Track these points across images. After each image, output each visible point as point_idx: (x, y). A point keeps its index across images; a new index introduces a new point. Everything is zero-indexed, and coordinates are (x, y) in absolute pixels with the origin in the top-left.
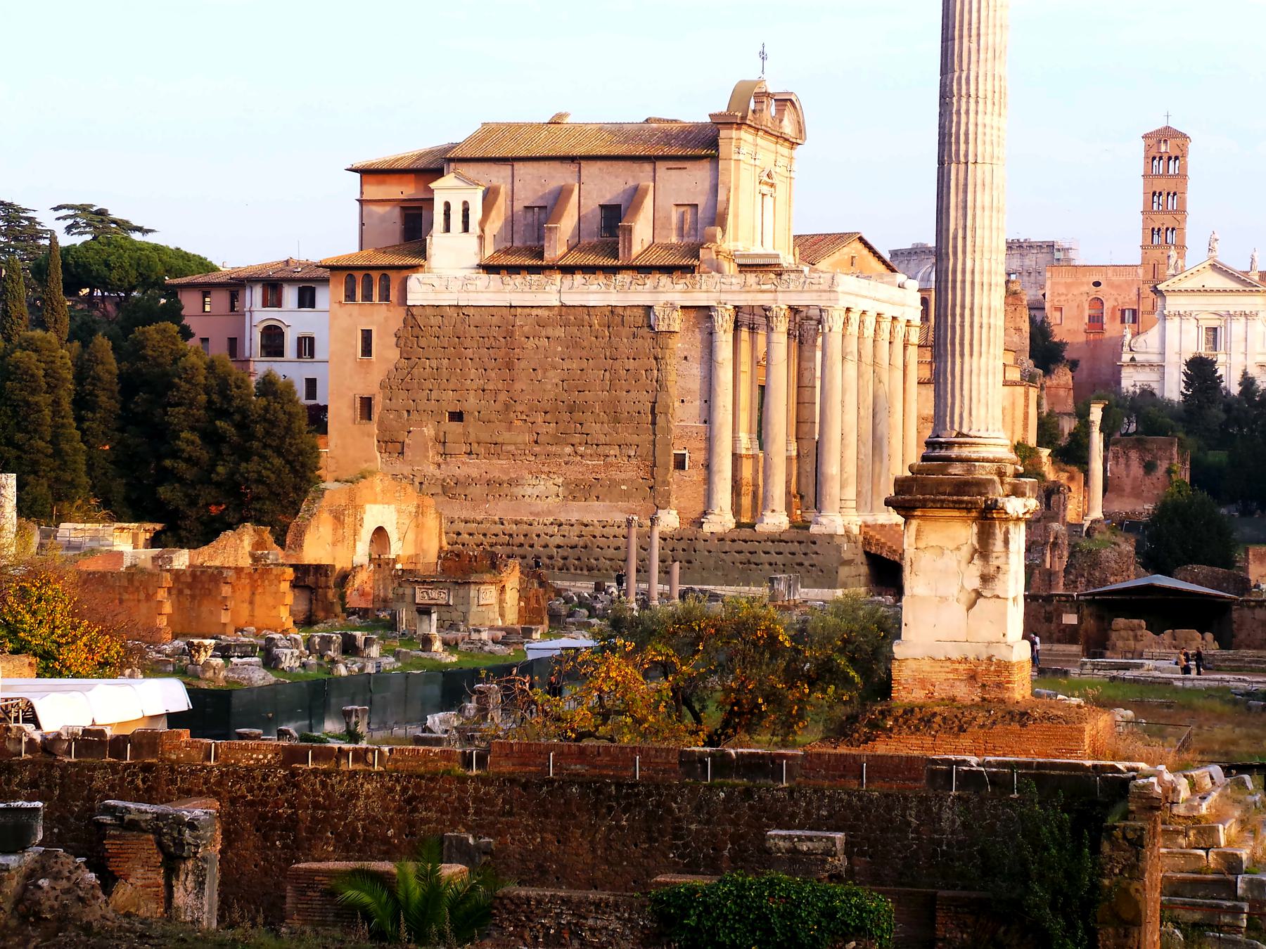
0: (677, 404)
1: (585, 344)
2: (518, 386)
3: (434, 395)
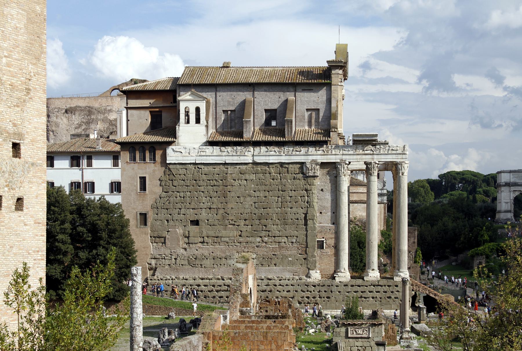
0: (318, 214)
1: (267, 183)
2: (230, 206)
3: (183, 211)
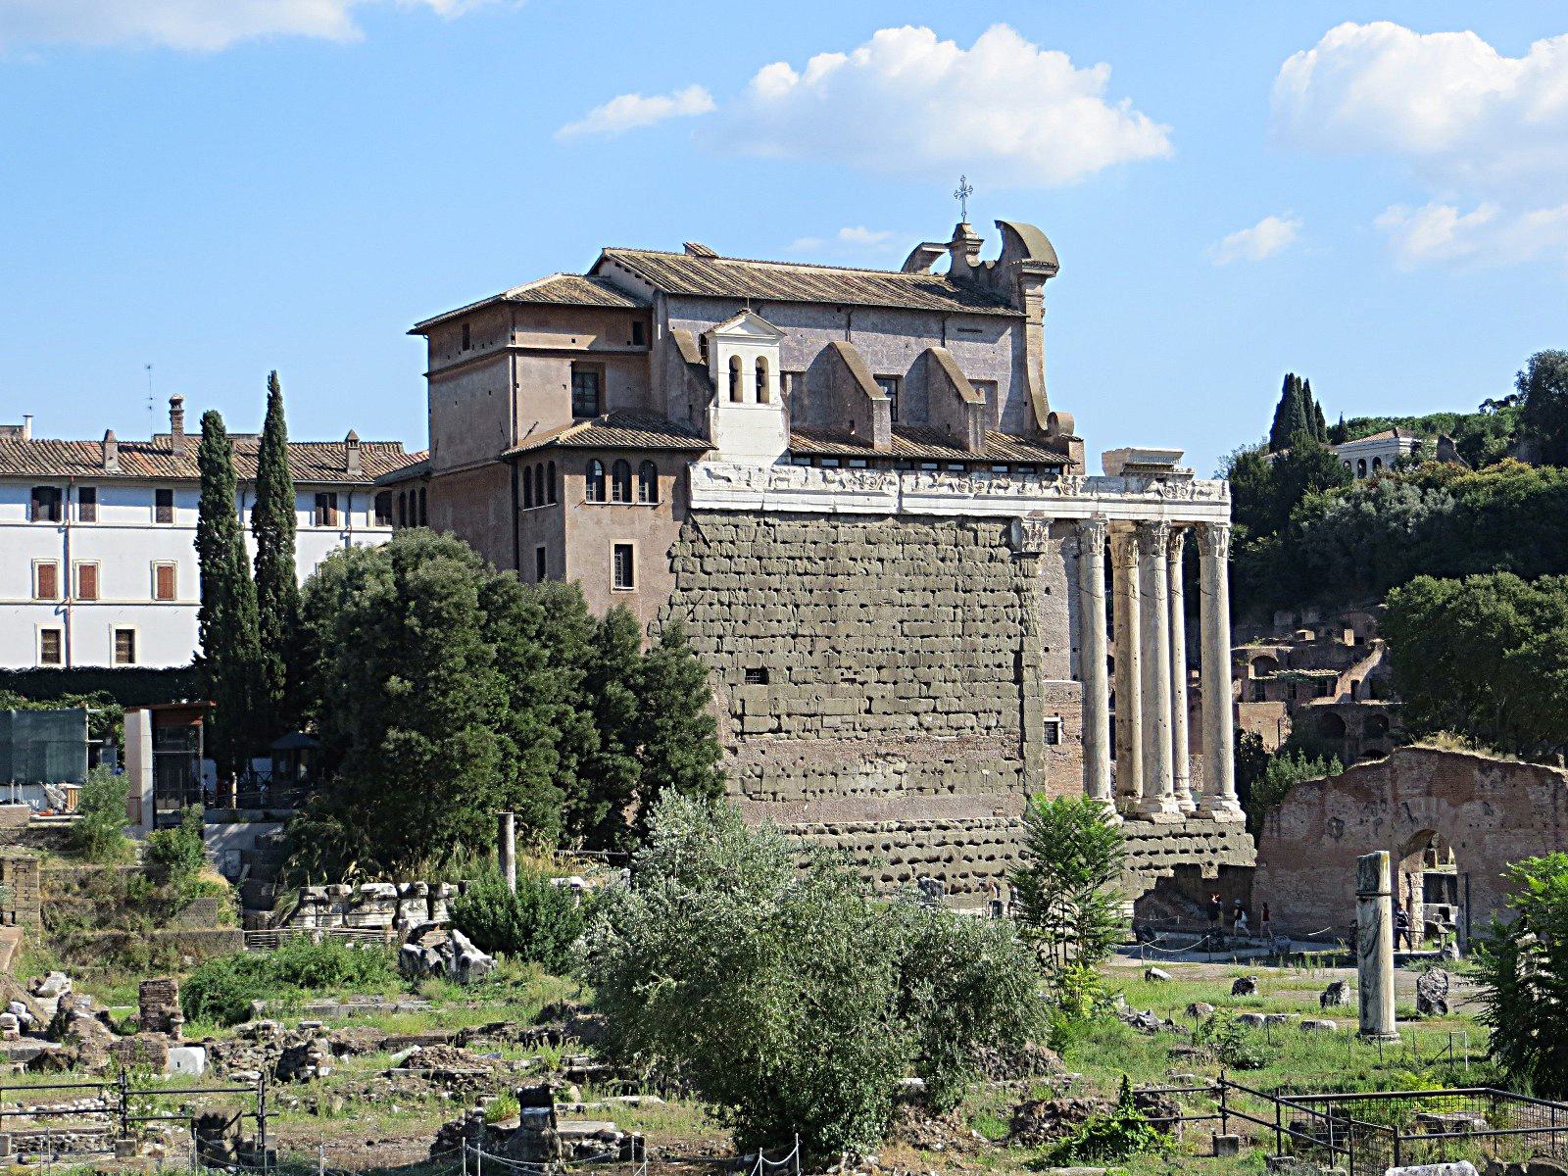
1: (931, 569)
2: (842, 628)
